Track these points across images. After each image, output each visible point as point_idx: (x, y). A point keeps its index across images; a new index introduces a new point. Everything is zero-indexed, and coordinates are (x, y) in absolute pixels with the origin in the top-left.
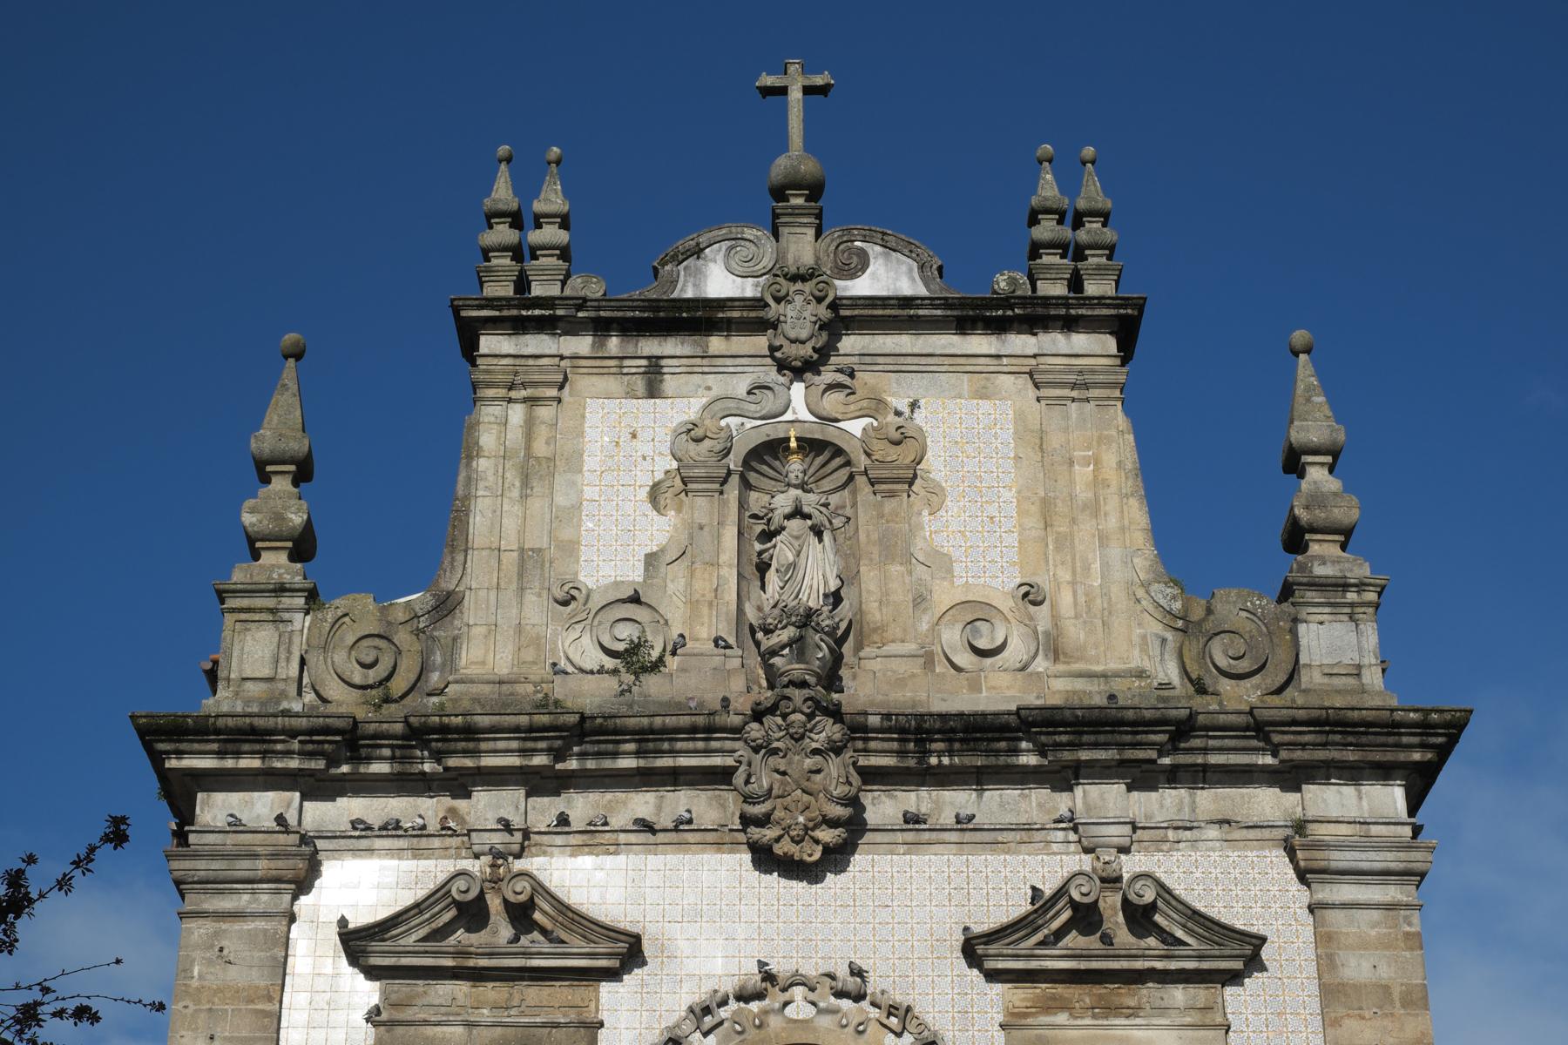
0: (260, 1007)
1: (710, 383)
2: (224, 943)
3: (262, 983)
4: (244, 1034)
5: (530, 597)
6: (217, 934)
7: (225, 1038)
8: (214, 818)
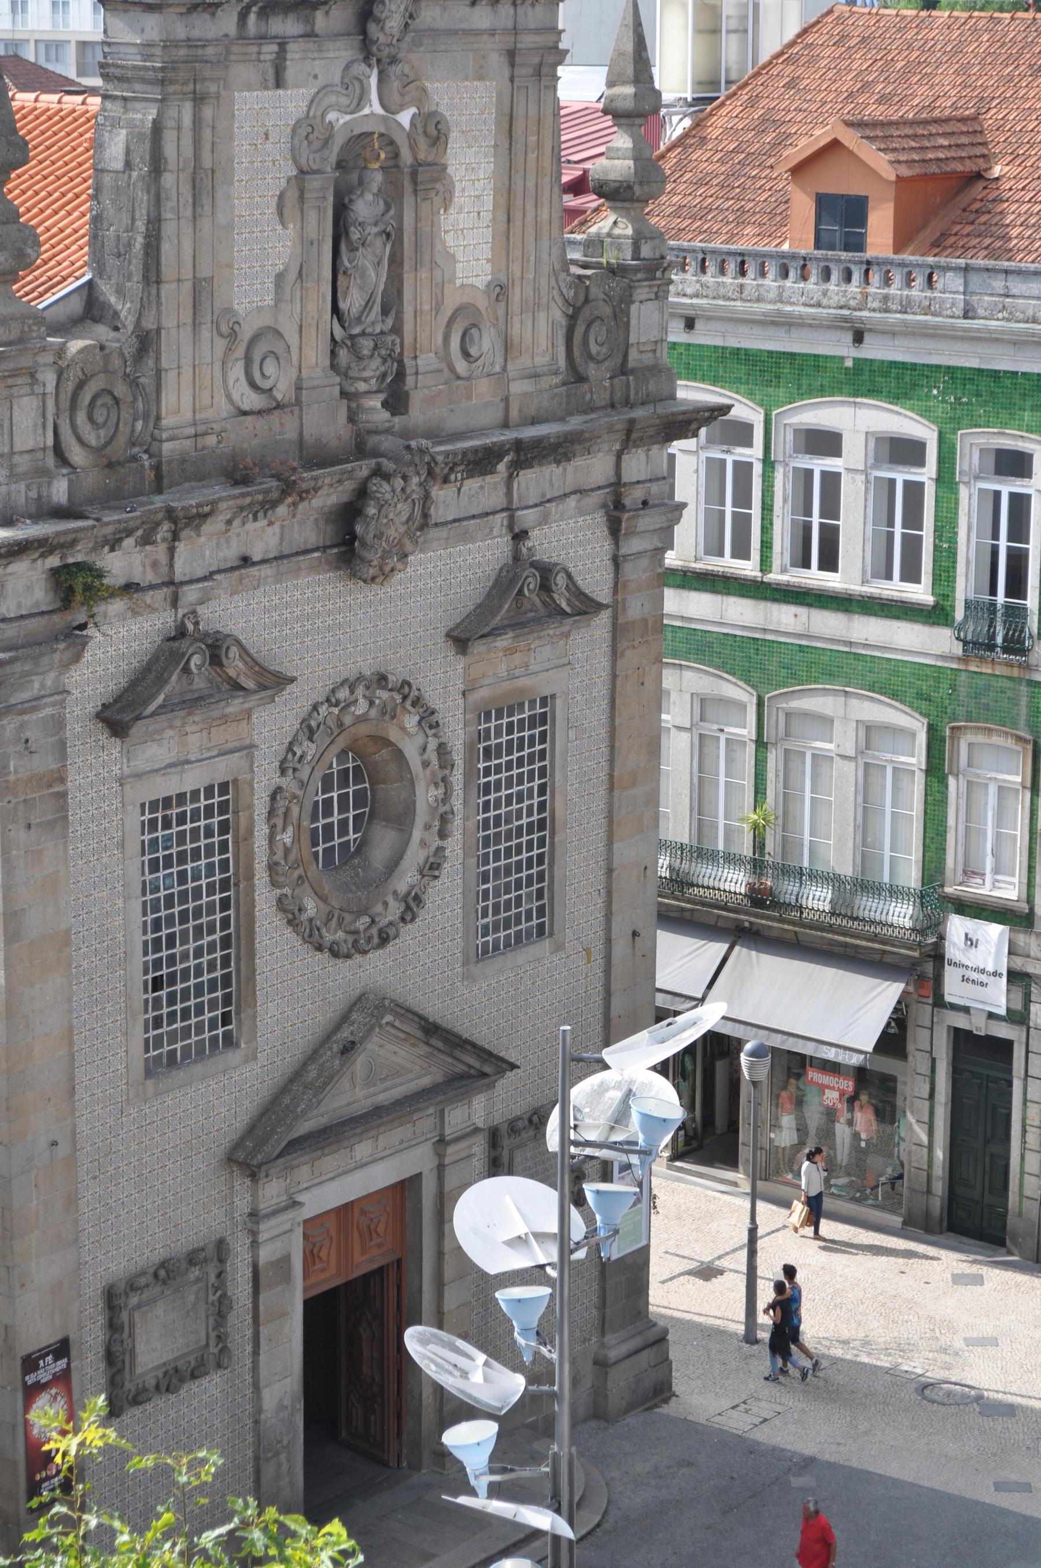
0: (56, 789)
1: (317, 71)
2: (28, 734)
3: (56, 766)
4: (50, 817)
5: (205, 333)
6: (22, 726)
7: (38, 825)
8: (8, 610)
